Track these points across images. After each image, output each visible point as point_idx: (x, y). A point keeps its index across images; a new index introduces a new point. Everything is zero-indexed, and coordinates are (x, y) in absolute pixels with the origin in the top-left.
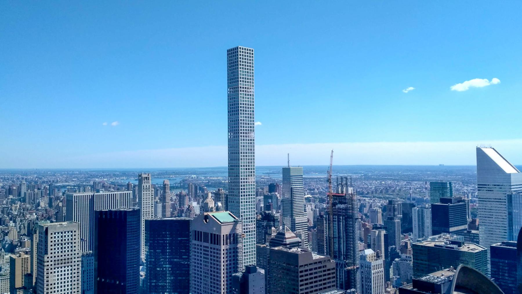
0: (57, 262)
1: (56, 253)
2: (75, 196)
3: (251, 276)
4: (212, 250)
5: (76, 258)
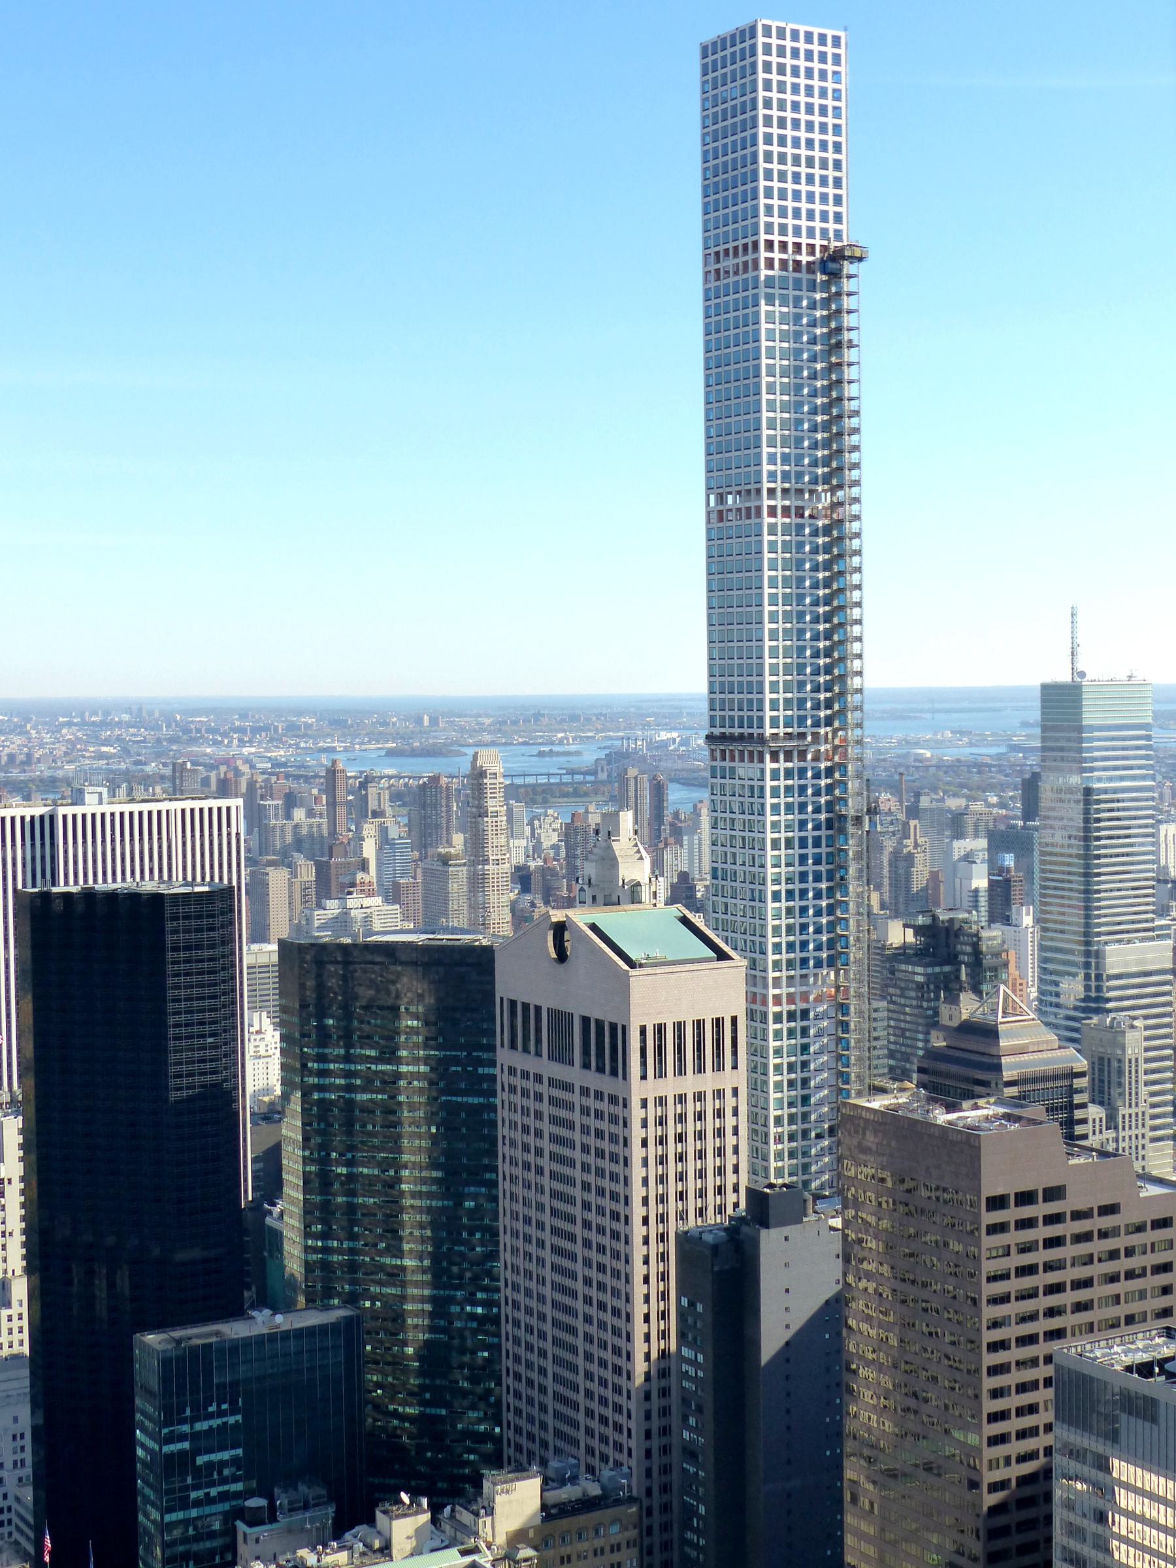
3: (771, 1241)
4: (590, 1102)
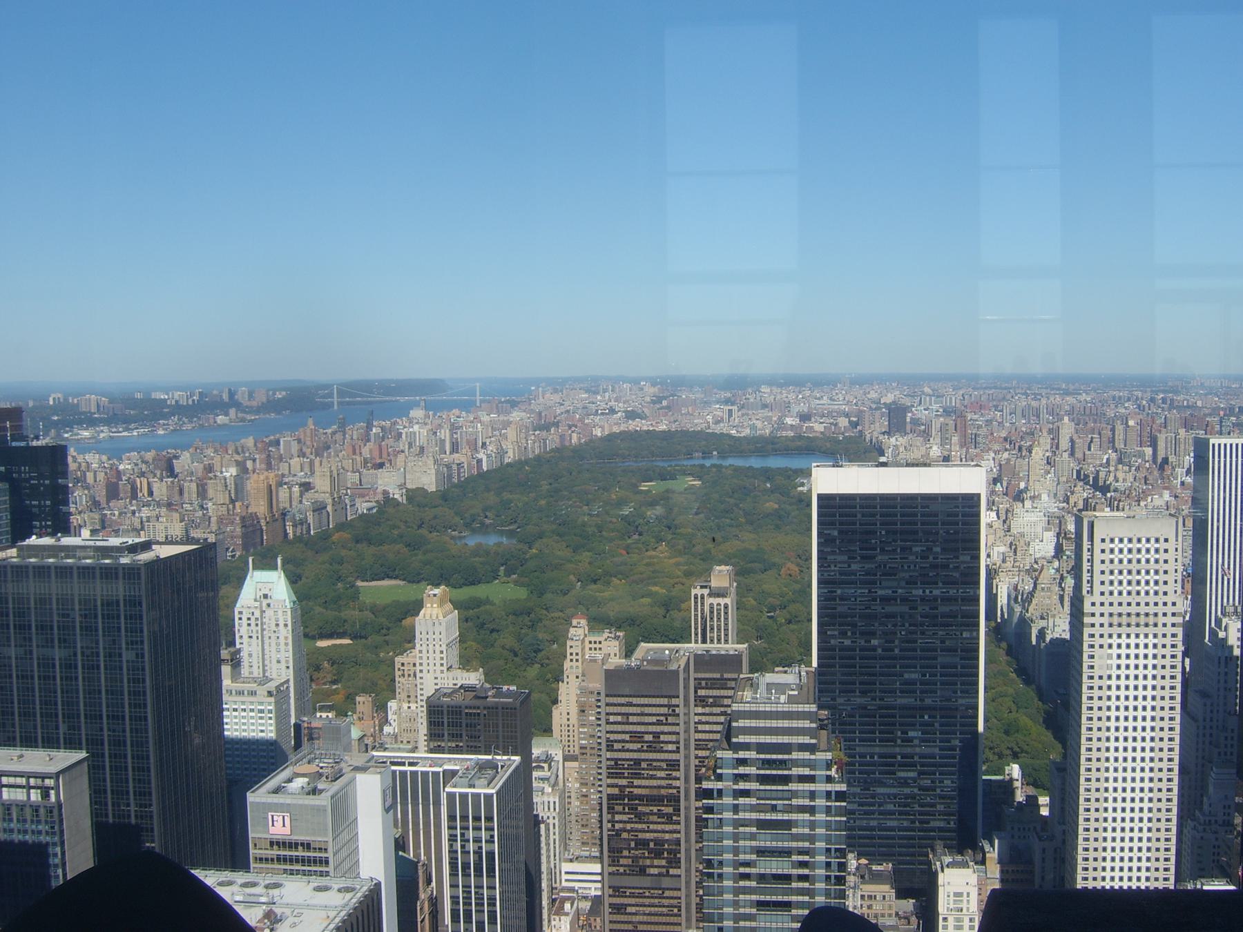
0: (1115, 620)
1: (1116, 593)
2: (1214, 445)
5: (1169, 614)
